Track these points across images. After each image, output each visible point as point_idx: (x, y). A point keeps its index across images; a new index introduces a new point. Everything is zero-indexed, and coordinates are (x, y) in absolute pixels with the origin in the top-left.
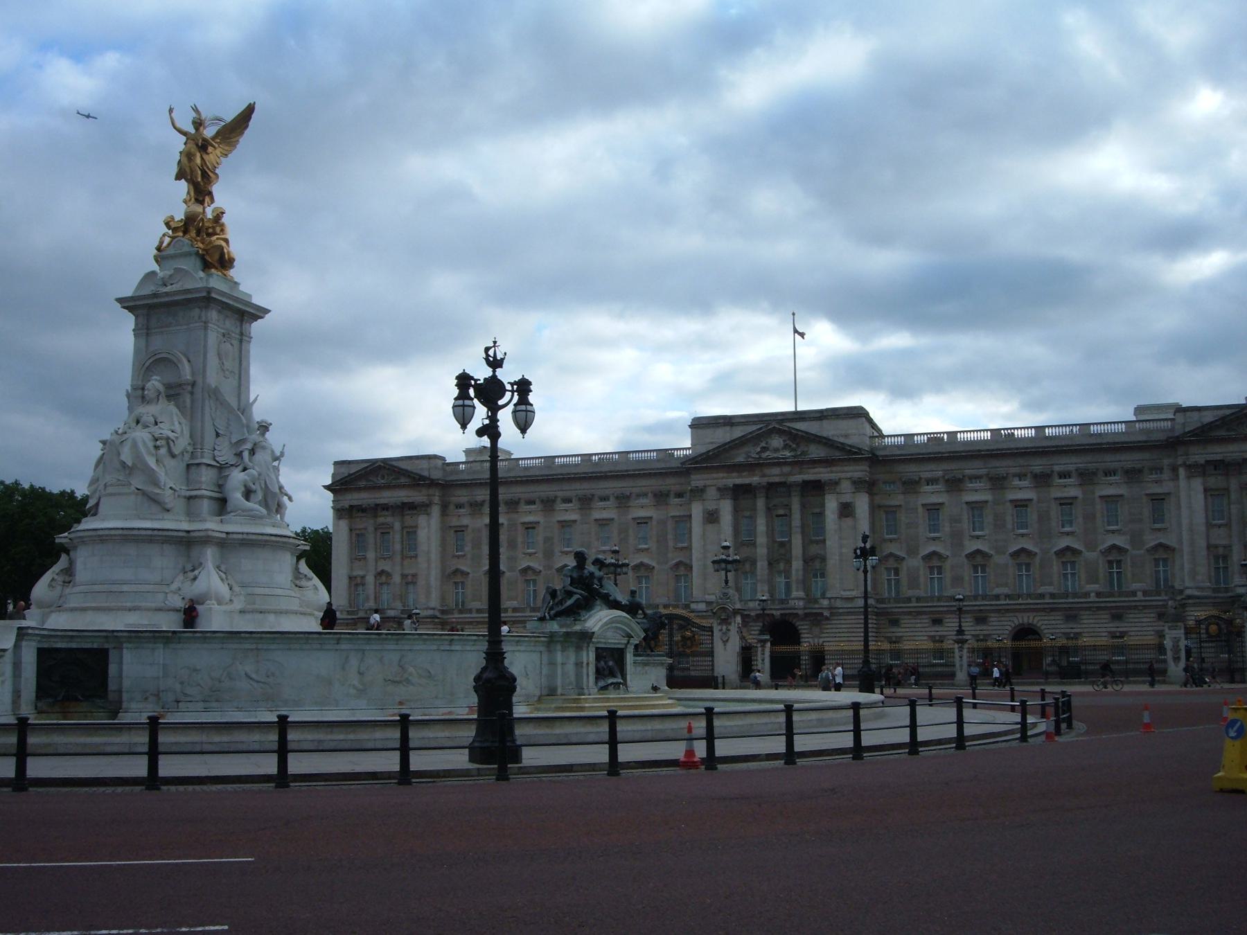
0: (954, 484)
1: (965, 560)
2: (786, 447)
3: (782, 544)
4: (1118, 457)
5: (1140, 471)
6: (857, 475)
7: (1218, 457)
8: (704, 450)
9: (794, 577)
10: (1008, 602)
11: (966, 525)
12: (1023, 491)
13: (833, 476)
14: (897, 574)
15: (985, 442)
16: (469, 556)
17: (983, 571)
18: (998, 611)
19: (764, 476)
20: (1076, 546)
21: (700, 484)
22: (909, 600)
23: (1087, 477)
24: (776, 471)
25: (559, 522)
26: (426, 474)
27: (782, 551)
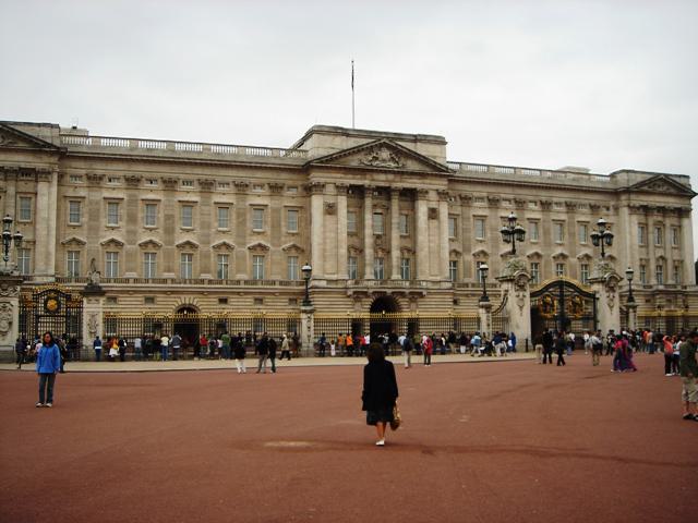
0: (494, 203)
3: (378, 237)
4: (589, 196)
5: (599, 207)
6: (442, 188)
7: (645, 204)
8: (326, 154)
12: (534, 212)
13: (425, 187)
14: (454, 266)
16: (85, 226)
19: (373, 180)
20: (566, 253)
21: (322, 180)
22: (467, 285)
23: (570, 207)
24: (382, 177)
26: (49, 141)
27: (379, 242)
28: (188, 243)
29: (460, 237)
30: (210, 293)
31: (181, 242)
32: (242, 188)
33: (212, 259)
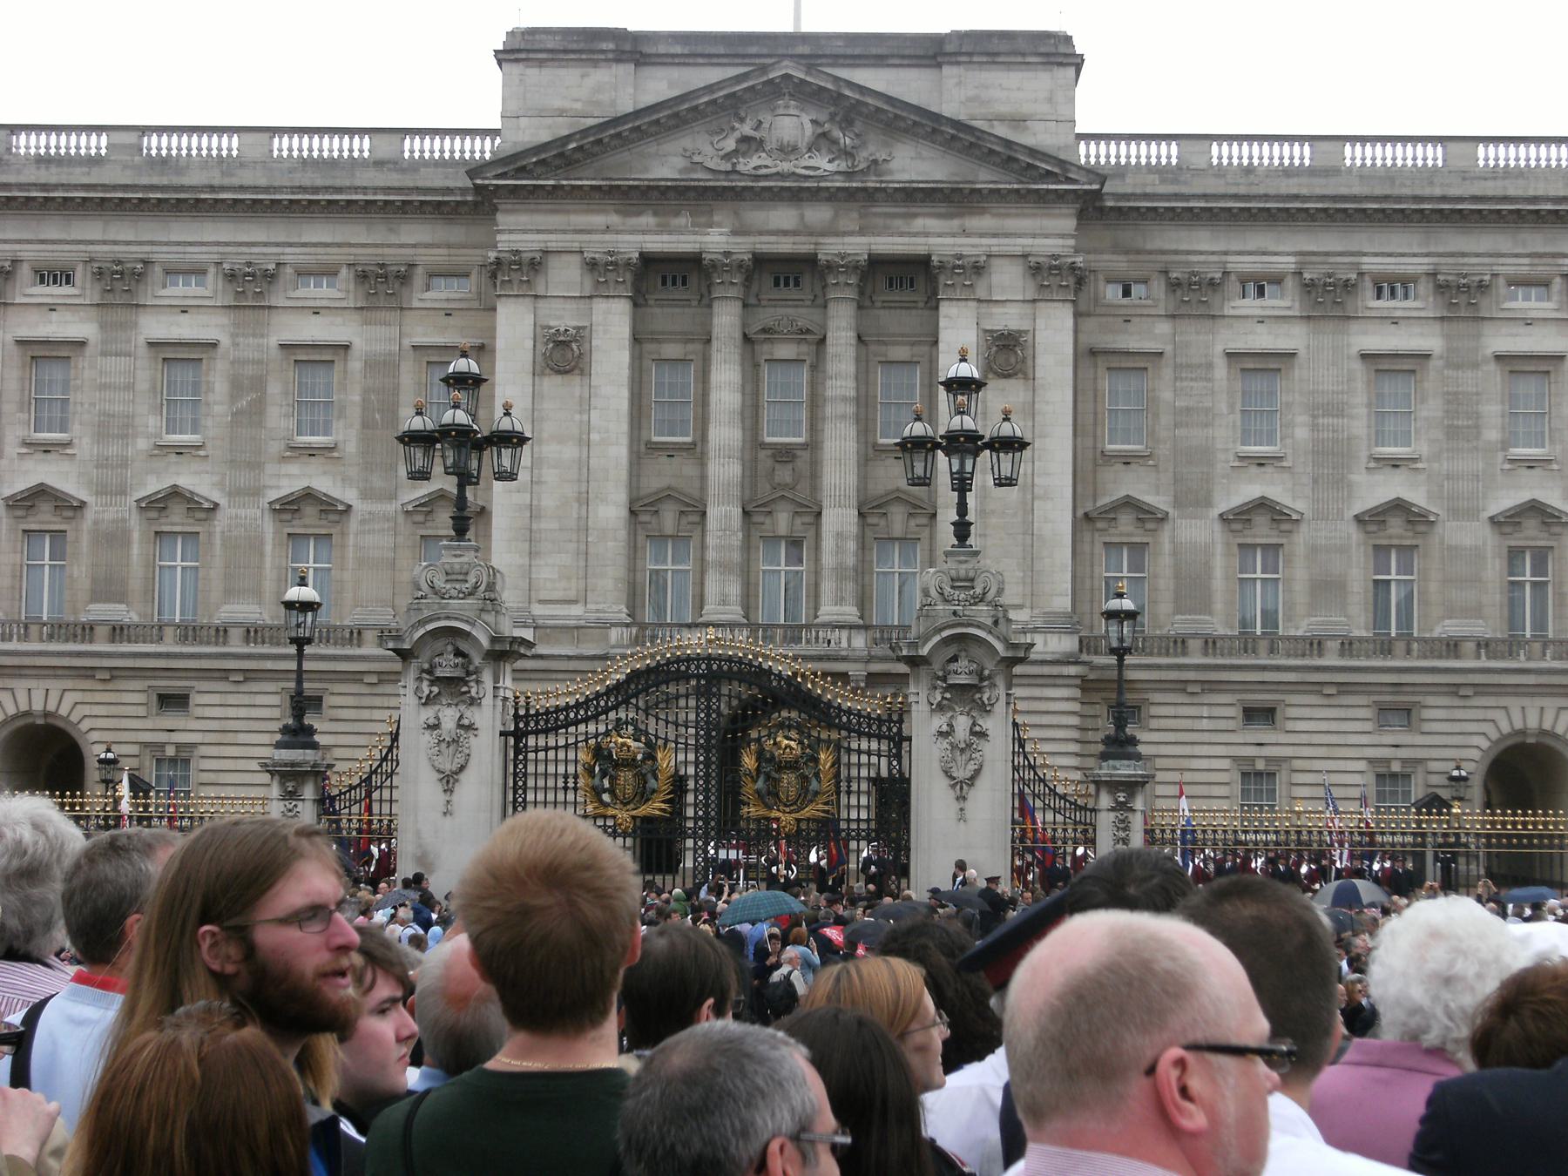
0: (1328, 297)
1: (1354, 533)
2: (822, 140)
3: (784, 454)
8: (545, 137)
9: (828, 559)
10: (1484, 663)
11: (1359, 425)
13: (971, 247)
14: (1136, 566)
15: (1430, 174)
17: (1405, 568)
18: (1454, 690)
24: (783, 216)
25: (21, 343)
27: (784, 474)
28: (41, 492)
29: (1164, 450)
30: (115, 674)
31: (21, 485)
32: (251, 286)
33: (135, 550)
